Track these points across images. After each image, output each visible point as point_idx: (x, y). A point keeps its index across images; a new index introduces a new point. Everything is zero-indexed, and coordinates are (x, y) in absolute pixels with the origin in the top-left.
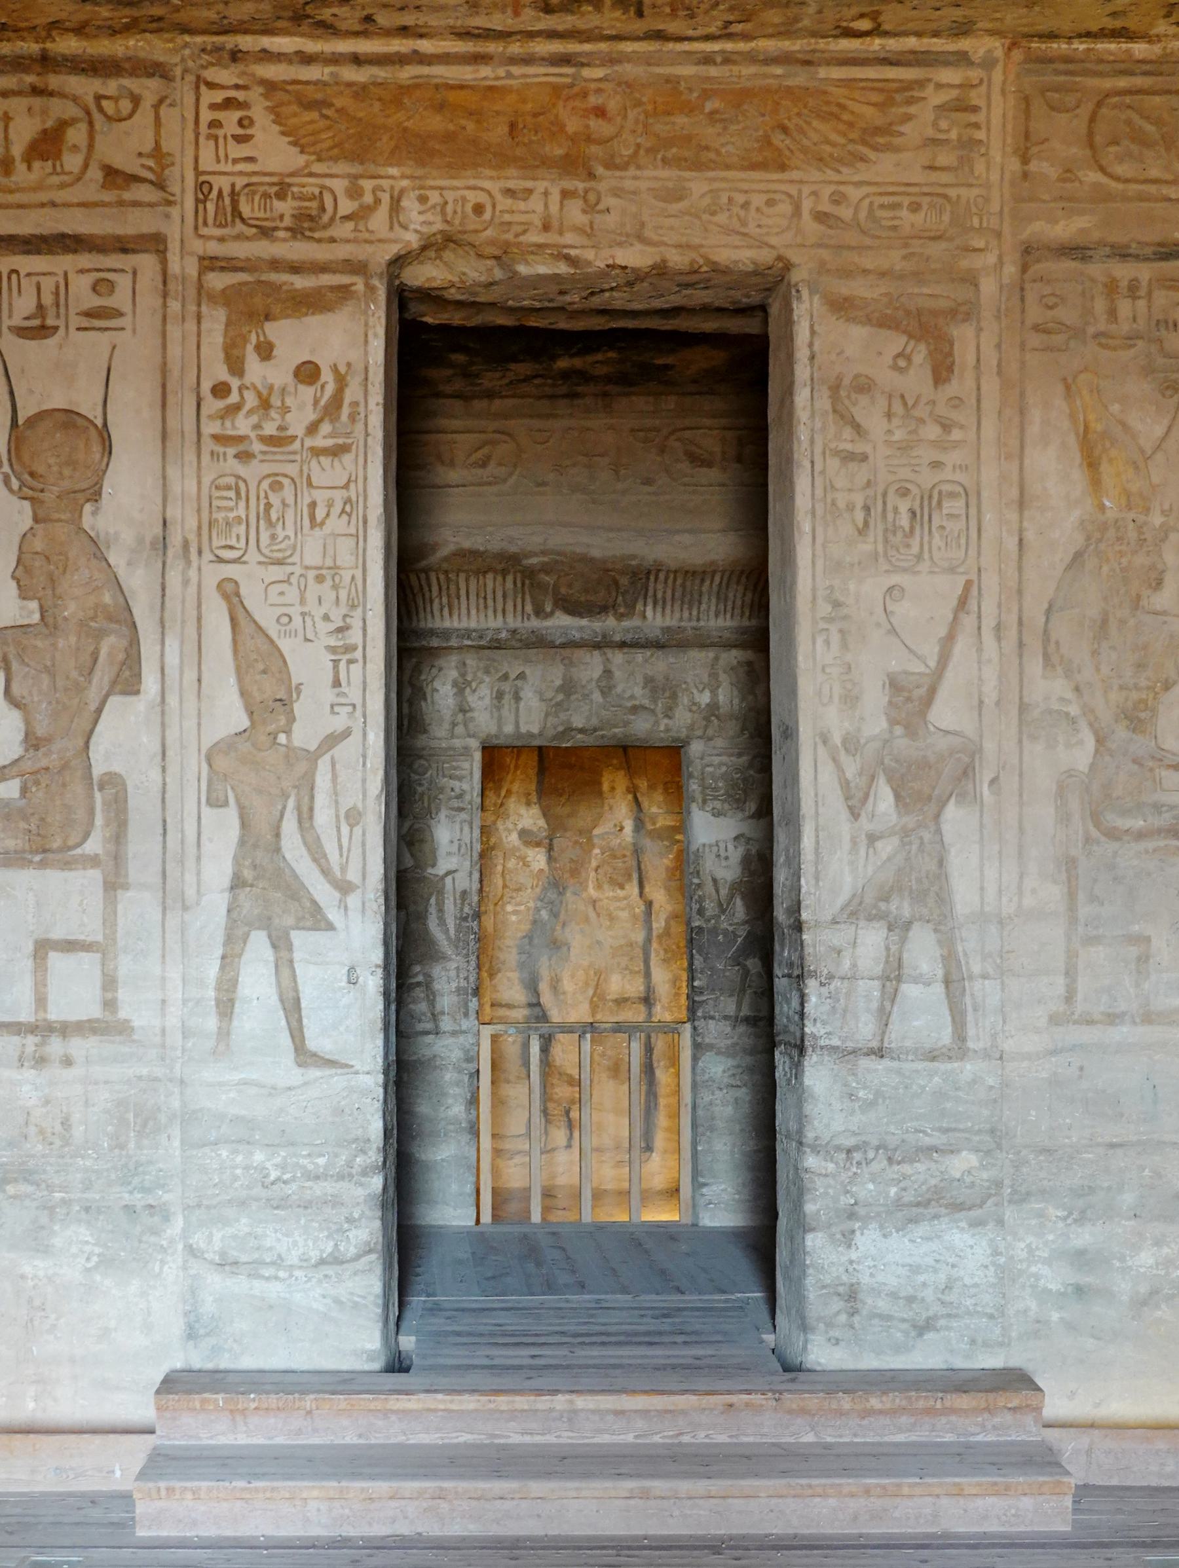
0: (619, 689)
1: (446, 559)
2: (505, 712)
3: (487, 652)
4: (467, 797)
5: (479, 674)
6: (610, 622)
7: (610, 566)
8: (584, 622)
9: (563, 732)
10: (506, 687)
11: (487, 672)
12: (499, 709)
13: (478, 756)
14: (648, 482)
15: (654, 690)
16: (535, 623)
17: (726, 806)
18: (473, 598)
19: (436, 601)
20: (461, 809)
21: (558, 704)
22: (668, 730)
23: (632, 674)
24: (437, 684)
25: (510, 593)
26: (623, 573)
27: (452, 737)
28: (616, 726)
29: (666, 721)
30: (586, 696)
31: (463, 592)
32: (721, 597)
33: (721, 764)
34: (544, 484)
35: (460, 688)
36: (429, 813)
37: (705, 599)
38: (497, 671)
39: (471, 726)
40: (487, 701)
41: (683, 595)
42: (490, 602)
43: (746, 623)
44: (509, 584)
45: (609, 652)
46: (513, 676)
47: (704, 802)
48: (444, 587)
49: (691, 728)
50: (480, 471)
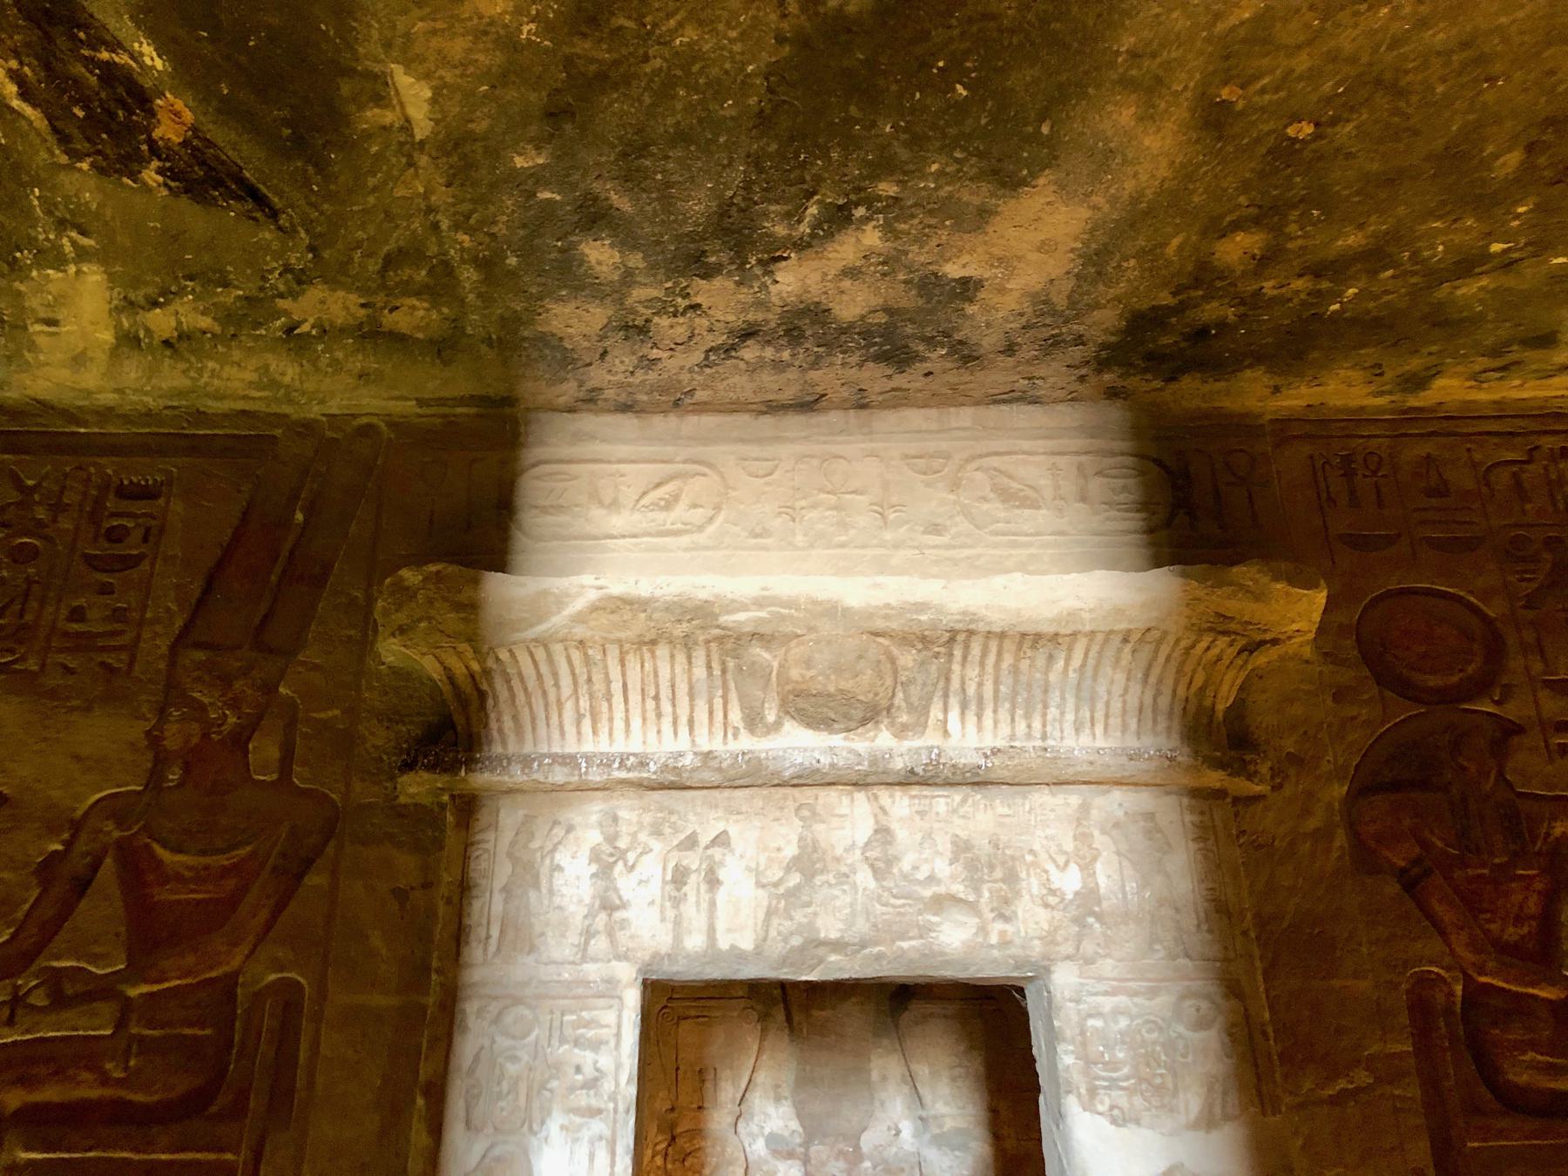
0: (906, 865)
1: (579, 618)
2: (689, 909)
3: (656, 795)
4: (607, 1086)
5: (643, 837)
6: (882, 740)
7: (880, 624)
8: (837, 740)
9: (802, 949)
10: (692, 860)
11: (657, 832)
12: (677, 902)
13: (632, 999)
14: (936, 529)
15: (972, 866)
16: (746, 742)
17: (1138, 1101)
18: (635, 697)
19: (569, 706)
20: (593, 1112)
21: (792, 893)
22: (1005, 943)
23: (929, 836)
24: (562, 857)
25: (702, 687)
26: (905, 640)
27: (584, 959)
28: (903, 937)
29: (999, 926)
30: (844, 877)
31: (616, 687)
32: (1085, 695)
33: (1117, 1012)
34: (765, 533)
35: (605, 863)
36: (530, 1122)
37: (1055, 698)
38: (676, 831)
39: (622, 937)
40: (655, 889)
41: (1015, 693)
42: (666, 707)
43: (1132, 742)
44: (700, 672)
45: (884, 795)
46: (704, 839)
47: (1093, 1092)
48: (582, 679)
49: (1049, 939)
50: (660, 516)
